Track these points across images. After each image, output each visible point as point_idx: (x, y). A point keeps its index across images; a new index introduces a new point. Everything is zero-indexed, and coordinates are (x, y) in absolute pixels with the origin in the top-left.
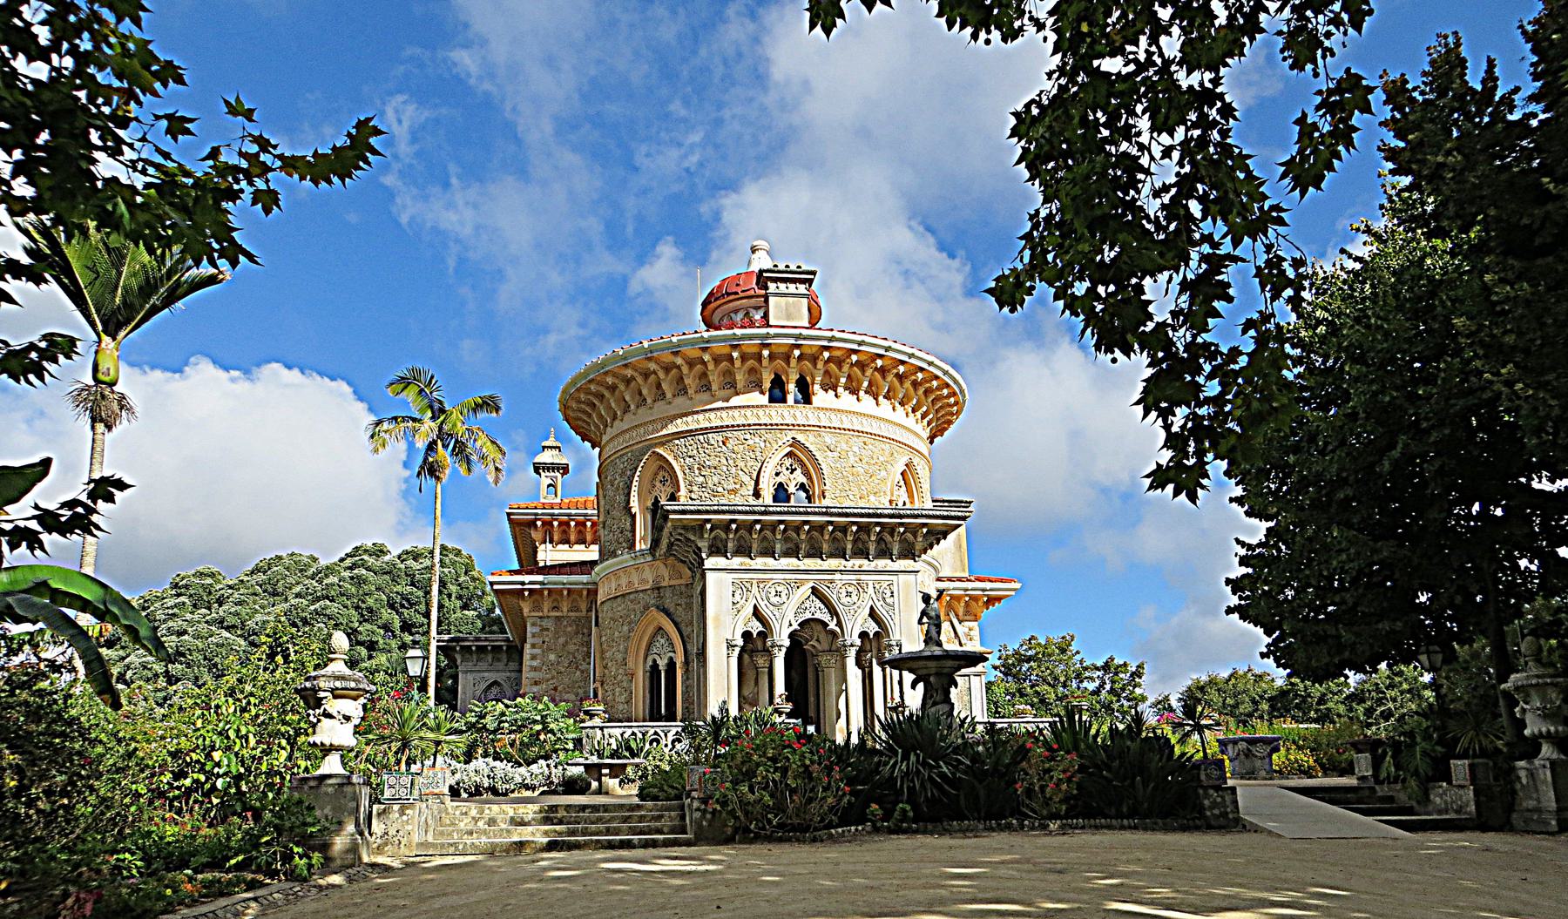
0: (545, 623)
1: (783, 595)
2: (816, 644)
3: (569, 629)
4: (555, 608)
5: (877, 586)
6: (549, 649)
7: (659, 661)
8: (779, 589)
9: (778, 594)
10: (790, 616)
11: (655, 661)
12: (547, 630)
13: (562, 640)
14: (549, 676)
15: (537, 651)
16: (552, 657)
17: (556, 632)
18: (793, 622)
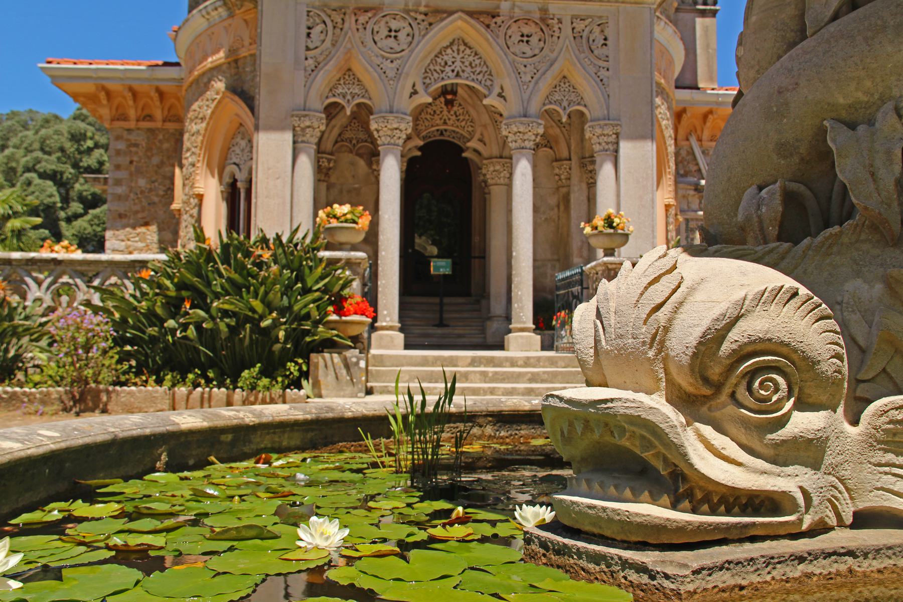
0: (133, 137)
1: (402, 35)
2: (479, 147)
3: (166, 145)
4: (149, 117)
5: (579, 26)
6: (139, 172)
7: (238, 176)
8: (394, 25)
9: (392, 33)
10: (413, 76)
11: (233, 176)
12: (136, 145)
13: (156, 160)
14: (137, 208)
15: (122, 174)
16: (142, 182)
17: (149, 149)
18: (420, 88)
